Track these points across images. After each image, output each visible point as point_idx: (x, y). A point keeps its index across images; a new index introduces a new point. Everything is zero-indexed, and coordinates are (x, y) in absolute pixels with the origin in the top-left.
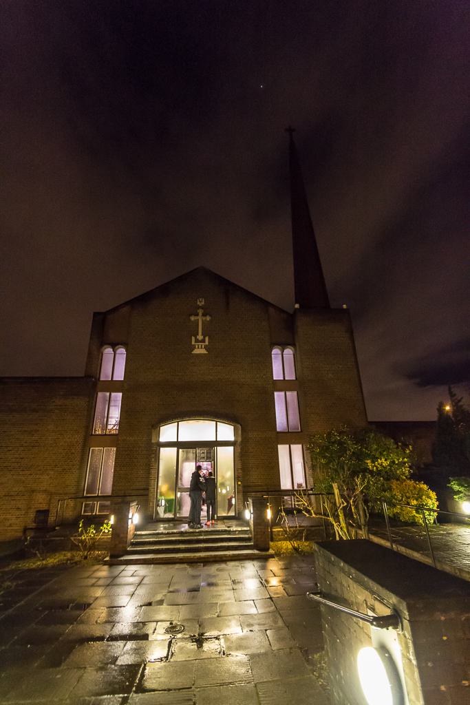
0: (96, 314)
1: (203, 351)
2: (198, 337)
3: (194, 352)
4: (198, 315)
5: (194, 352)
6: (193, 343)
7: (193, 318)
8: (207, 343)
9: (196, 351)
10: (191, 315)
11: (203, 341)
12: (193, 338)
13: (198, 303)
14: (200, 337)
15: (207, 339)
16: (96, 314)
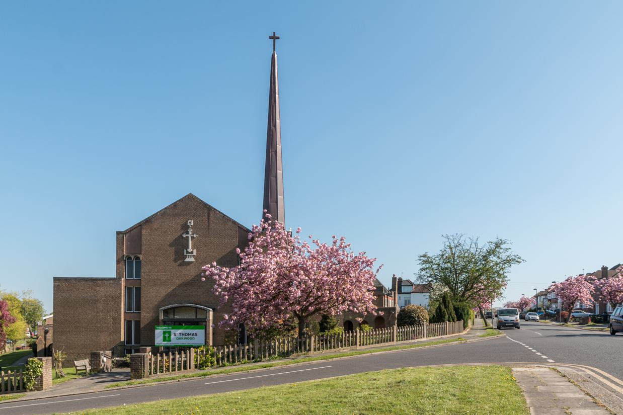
0: (118, 233)
1: (192, 260)
2: (188, 250)
3: (186, 260)
4: (187, 233)
5: (186, 260)
6: (185, 254)
7: (184, 236)
8: (195, 254)
9: (188, 260)
10: (183, 234)
11: (192, 253)
12: (185, 251)
13: (188, 224)
14: (190, 250)
15: (195, 251)
16: (118, 233)
